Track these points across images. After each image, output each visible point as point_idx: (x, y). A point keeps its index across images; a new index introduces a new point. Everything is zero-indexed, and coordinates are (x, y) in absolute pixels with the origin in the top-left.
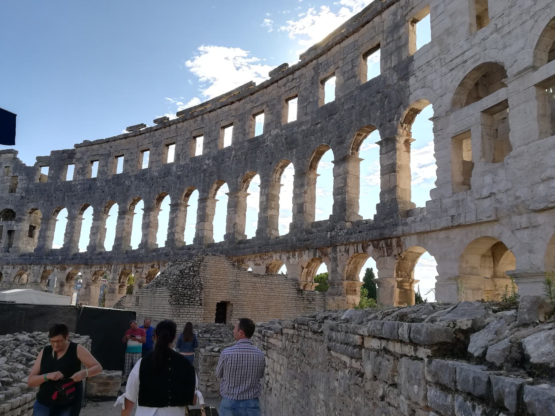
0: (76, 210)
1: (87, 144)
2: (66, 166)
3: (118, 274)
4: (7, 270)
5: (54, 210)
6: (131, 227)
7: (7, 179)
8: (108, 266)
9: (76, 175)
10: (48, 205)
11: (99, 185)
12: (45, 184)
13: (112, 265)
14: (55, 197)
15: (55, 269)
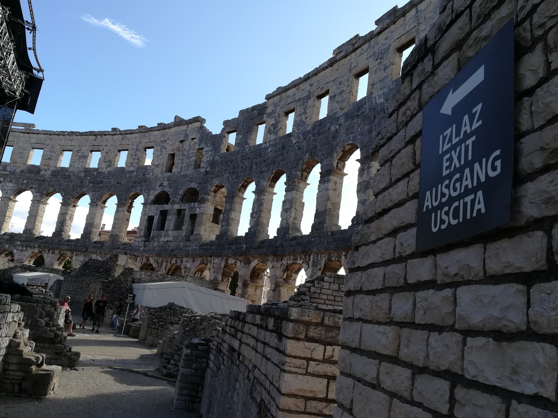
0: (264, 181)
1: (281, 91)
2: (255, 127)
3: (320, 269)
4: (186, 264)
5: (240, 185)
6: (339, 195)
7: (193, 153)
8: (305, 256)
9: (267, 135)
10: (233, 179)
11: (294, 141)
12: (232, 153)
13: (310, 255)
14: (242, 167)
15: (238, 262)
